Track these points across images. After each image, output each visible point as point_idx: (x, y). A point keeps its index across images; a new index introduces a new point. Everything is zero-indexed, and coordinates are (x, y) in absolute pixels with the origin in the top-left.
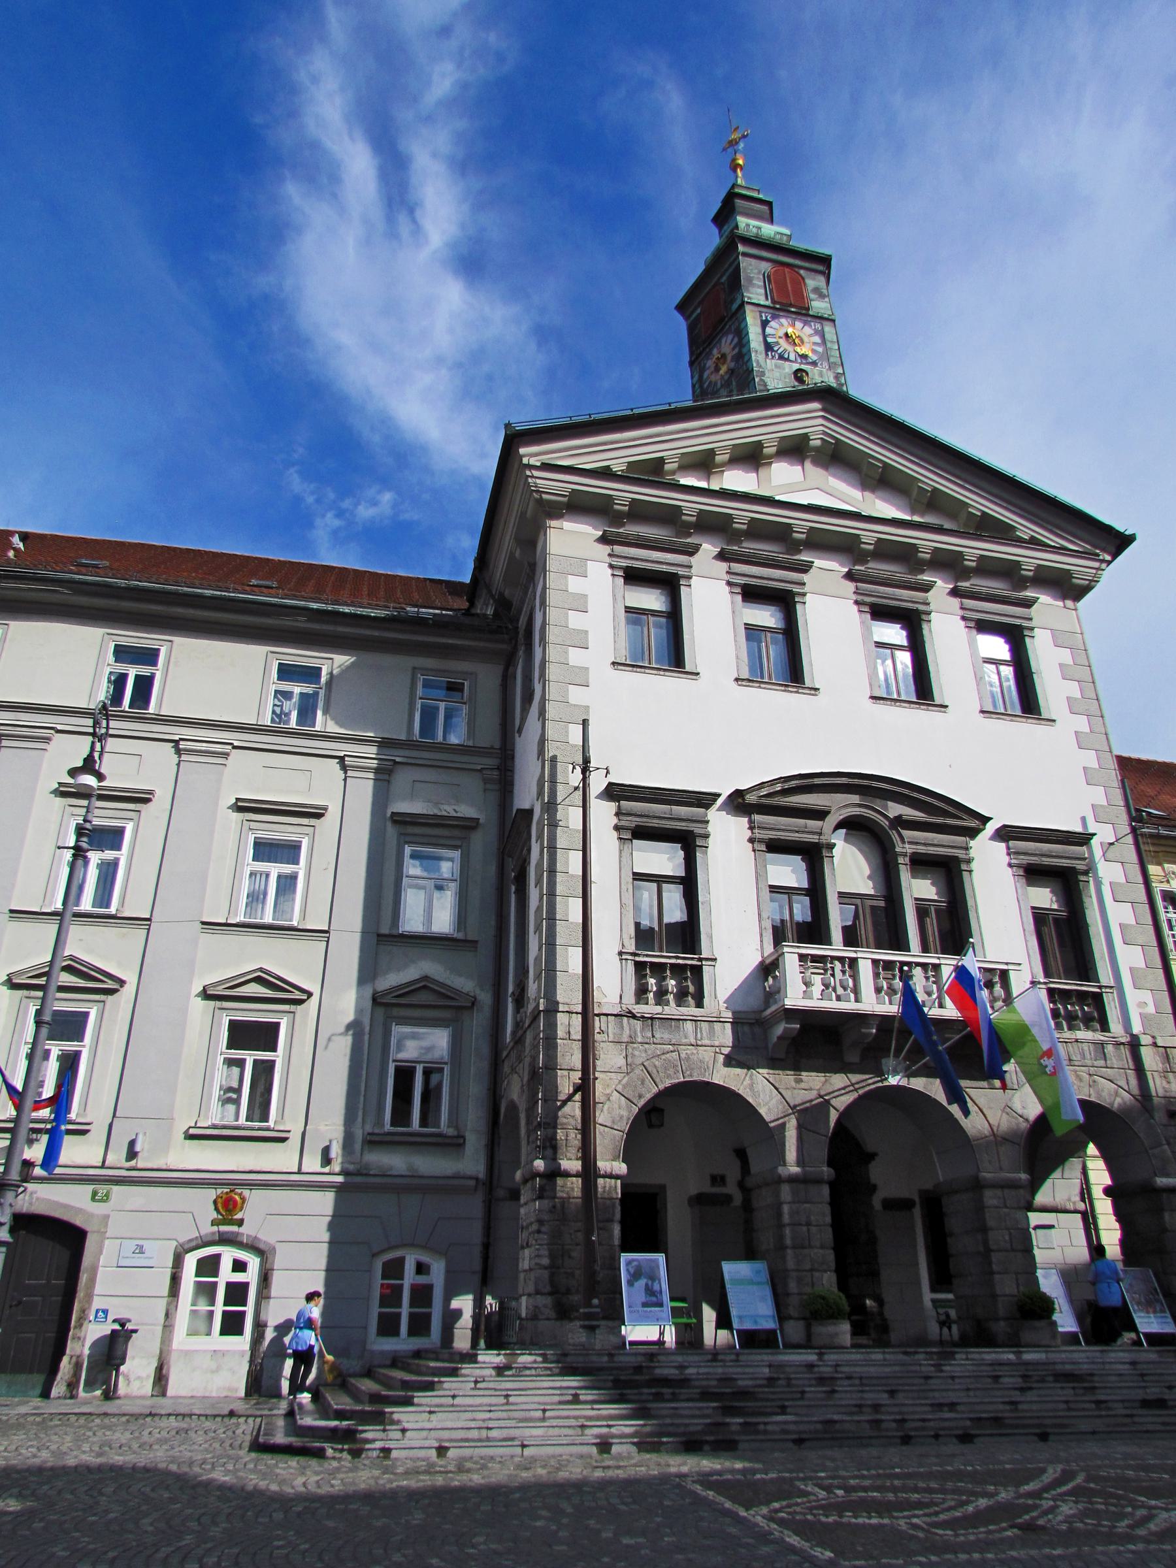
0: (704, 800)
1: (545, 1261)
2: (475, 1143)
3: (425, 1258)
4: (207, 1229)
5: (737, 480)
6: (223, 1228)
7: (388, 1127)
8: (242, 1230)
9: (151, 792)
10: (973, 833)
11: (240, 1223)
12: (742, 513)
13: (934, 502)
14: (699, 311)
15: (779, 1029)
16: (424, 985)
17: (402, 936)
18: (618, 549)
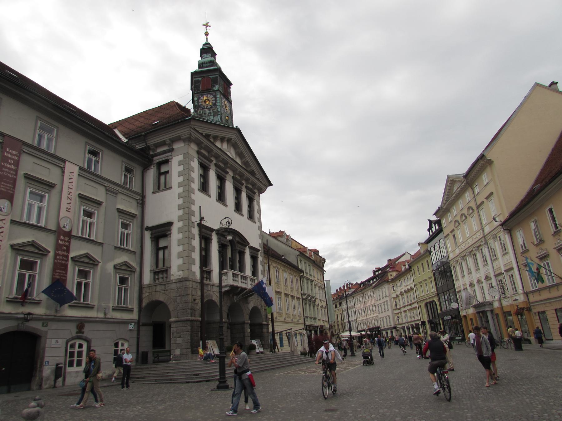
0: (212, 230)
1: (190, 341)
2: (136, 310)
3: (123, 342)
4: (74, 334)
5: (218, 144)
6: (79, 334)
7: (116, 305)
8: (83, 335)
9: (55, 185)
10: (246, 246)
11: (83, 333)
12: (223, 156)
13: (246, 164)
14: (200, 79)
15: (227, 289)
16: (126, 264)
17: (119, 248)
18: (200, 157)
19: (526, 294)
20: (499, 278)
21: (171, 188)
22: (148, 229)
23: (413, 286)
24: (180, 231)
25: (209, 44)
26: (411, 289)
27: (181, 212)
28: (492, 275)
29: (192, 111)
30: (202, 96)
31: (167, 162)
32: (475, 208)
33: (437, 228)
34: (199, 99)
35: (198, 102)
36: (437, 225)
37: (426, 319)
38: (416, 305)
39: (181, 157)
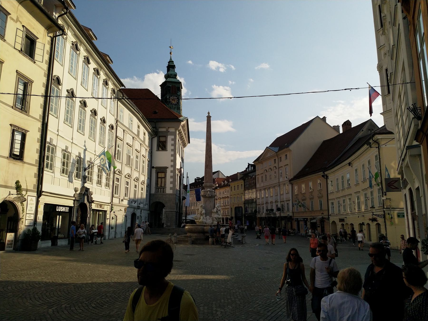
14: (170, 86)
19: (293, 213)
20: (282, 203)
21: (167, 151)
22: (153, 167)
23: (229, 196)
24: (171, 172)
25: (173, 62)
26: (228, 197)
27: (172, 163)
28: (279, 201)
29: (160, 98)
30: (171, 96)
31: (166, 137)
32: (277, 167)
33: (252, 169)
34: (170, 97)
35: (169, 99)
36: (252, 167)
37: (233, 215)
38: (229, 207)
39: (173, 137)
